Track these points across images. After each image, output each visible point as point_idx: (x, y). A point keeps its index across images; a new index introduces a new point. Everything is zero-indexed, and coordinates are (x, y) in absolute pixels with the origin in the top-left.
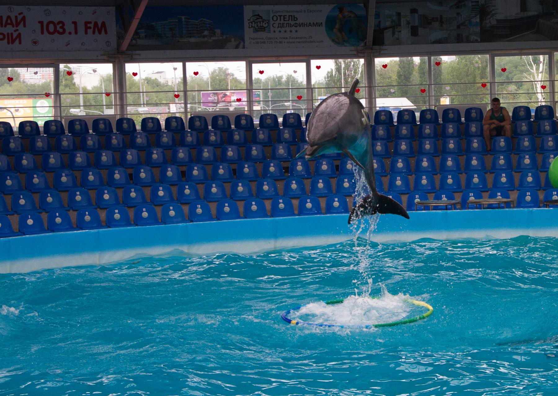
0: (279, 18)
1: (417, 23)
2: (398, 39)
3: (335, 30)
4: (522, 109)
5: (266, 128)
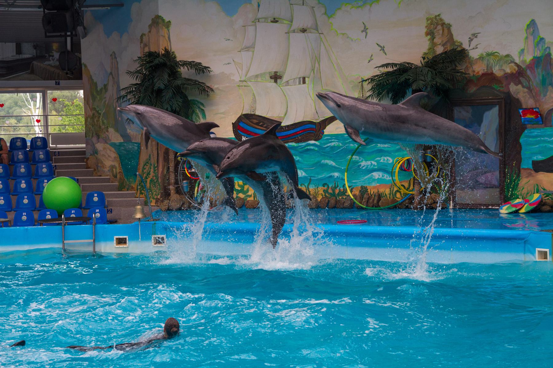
4: (19, 140)
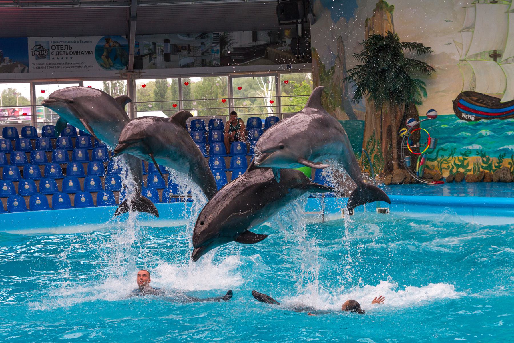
0: (57, 47)
1: (169, 51)
2: (154, 64)
3: (102, 57)
5: (48, 137)
